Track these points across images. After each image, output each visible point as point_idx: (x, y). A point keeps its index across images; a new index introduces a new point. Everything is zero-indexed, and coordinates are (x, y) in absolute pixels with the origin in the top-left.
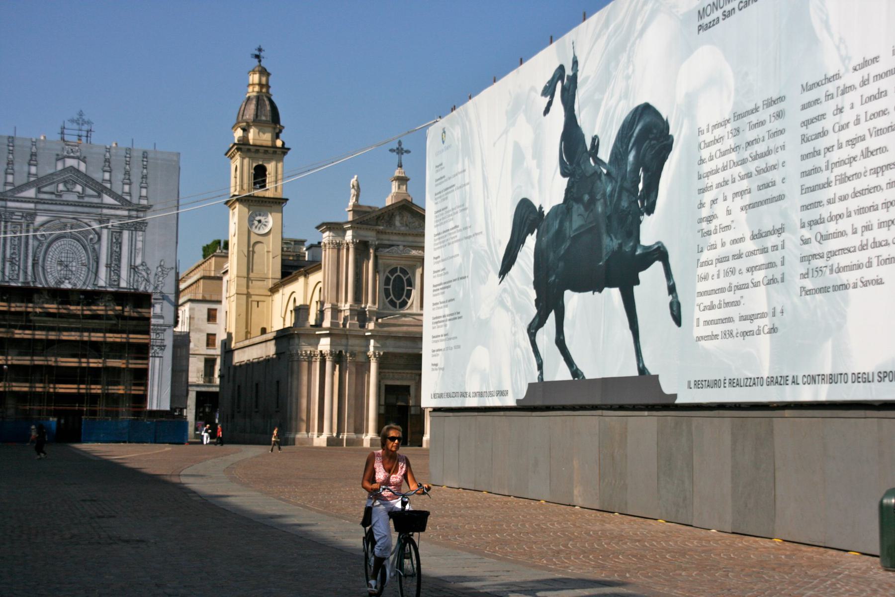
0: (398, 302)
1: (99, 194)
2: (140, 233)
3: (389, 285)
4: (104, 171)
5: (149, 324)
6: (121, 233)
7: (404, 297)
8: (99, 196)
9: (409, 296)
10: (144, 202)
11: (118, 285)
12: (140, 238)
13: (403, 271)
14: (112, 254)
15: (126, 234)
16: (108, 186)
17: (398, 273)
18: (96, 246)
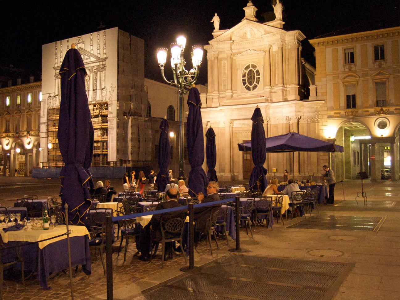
0: (251, 87)
1: (89, 57)
2: (104, 72)
3: (245, 77)
4: (91, 46)
5: (108, 119)
6: (97, 74)
7: (255, 83)
8: (89, 58)
9: (258, 82)
10: (105, 56)
11: (96, 100)
12: (104, 75)
13: (254, 67)
14: (94, 85)
15: (99, 73)
16: (92, 52)
17: (251, 68)
18: (88, 83)
